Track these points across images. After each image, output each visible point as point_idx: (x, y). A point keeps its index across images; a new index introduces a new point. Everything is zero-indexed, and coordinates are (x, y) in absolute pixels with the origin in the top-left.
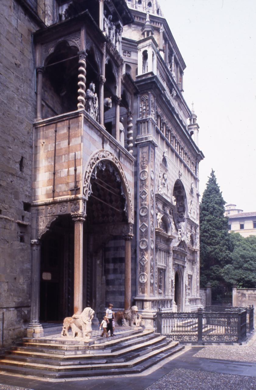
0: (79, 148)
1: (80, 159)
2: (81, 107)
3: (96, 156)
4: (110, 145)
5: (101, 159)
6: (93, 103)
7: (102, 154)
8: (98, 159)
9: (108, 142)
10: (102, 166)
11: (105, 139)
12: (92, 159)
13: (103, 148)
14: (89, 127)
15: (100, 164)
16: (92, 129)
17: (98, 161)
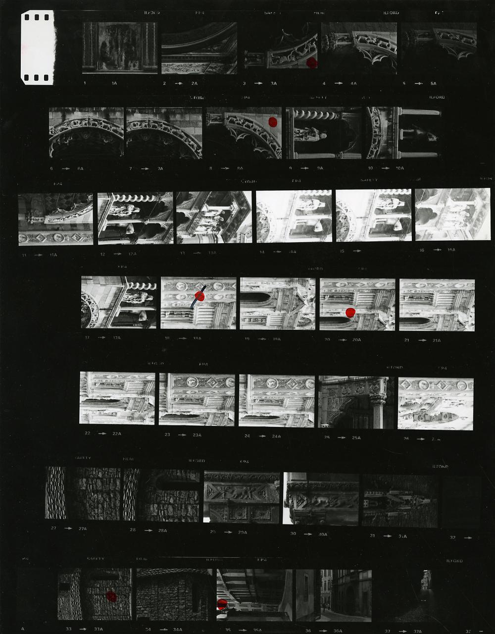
0: (96, 282)
1: (86, 283)
2: (130, 285)
3: (91, 301)
4: (105, 318)
5: (90, 306)
6: (136, 298)
7: (95, 308)
8: (90, 303)
9: (107, 316)
10: (84, 309)
11: (110, 312)
12: (89, 296)
13: (101, 309)
14: (116, 294)
15: (85, 306)
16: (114, 297)
17: (88, 304)
